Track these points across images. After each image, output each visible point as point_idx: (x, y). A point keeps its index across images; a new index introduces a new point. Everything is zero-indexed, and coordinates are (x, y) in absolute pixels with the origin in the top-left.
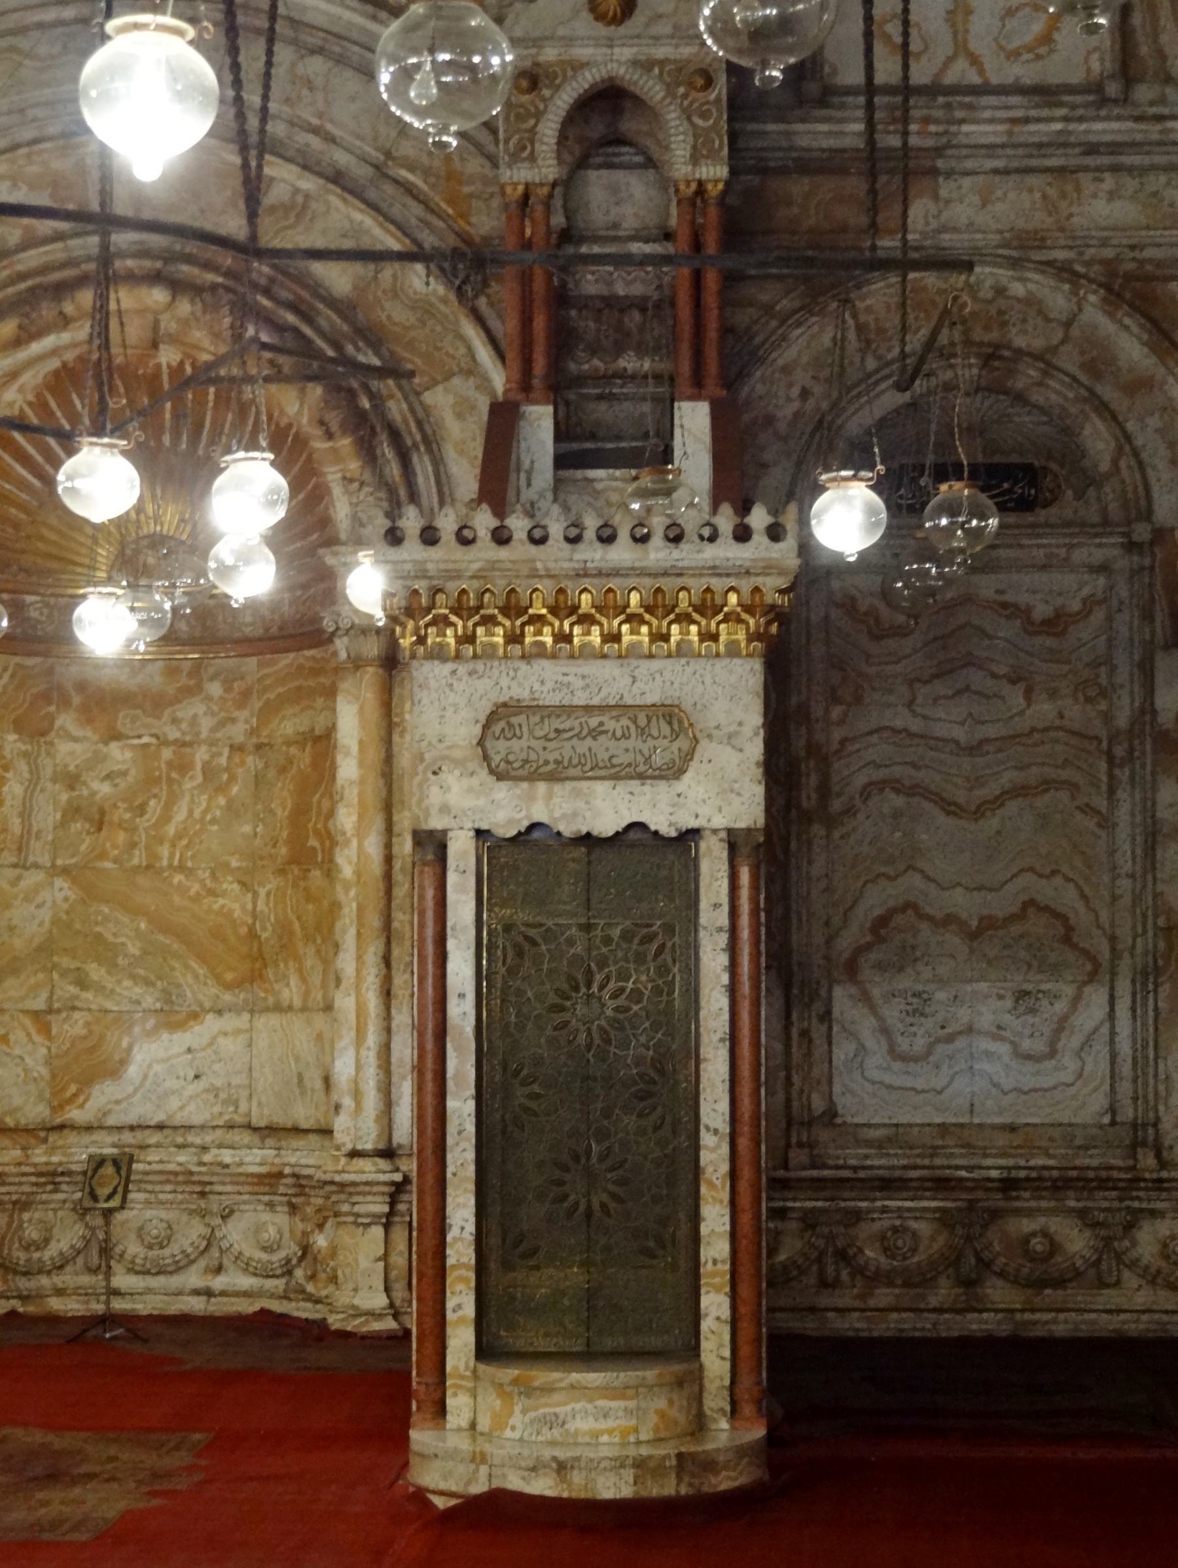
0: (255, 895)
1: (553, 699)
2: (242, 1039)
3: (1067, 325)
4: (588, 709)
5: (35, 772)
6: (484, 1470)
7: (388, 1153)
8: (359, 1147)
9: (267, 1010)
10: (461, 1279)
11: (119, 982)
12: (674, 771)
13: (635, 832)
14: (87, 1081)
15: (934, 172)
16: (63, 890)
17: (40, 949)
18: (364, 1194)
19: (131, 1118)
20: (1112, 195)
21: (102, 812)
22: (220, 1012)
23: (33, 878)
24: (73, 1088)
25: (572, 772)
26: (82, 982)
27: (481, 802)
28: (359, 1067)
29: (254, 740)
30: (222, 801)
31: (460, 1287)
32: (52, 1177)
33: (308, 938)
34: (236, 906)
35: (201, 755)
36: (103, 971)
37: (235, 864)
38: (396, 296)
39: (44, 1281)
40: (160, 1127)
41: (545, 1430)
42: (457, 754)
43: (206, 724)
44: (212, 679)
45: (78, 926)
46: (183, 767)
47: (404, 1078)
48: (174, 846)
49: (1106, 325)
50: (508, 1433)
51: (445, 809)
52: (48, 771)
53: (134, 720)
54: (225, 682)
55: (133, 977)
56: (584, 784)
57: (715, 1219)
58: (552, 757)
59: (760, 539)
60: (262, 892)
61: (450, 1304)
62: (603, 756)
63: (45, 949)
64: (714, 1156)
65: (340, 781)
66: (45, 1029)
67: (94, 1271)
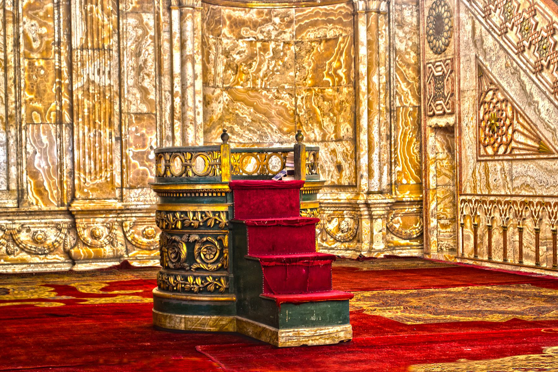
0: (296, 99)
7: (381, 192)
8: (373, 190)
11: (244, 132)
16: (226, 97)
18: (376, 207)
21: (237, 67)
23: (218, 91)
28: (370, 160)
29: (294, 40)
30: (281, 63)
33: (324, 115)
34: (288, 103)
35: (272, 45)
36: (239, 128)
37: (287, 86)
43: (274, 34)
44: (276, 16)
45: (230, 110)
46: (265, 49)
47: (384, 165)
48: (262, 80)
52: (220, 51)
54: (281, 18)
55: (250, 130)
60: (299, 97)
65: (360, 56)
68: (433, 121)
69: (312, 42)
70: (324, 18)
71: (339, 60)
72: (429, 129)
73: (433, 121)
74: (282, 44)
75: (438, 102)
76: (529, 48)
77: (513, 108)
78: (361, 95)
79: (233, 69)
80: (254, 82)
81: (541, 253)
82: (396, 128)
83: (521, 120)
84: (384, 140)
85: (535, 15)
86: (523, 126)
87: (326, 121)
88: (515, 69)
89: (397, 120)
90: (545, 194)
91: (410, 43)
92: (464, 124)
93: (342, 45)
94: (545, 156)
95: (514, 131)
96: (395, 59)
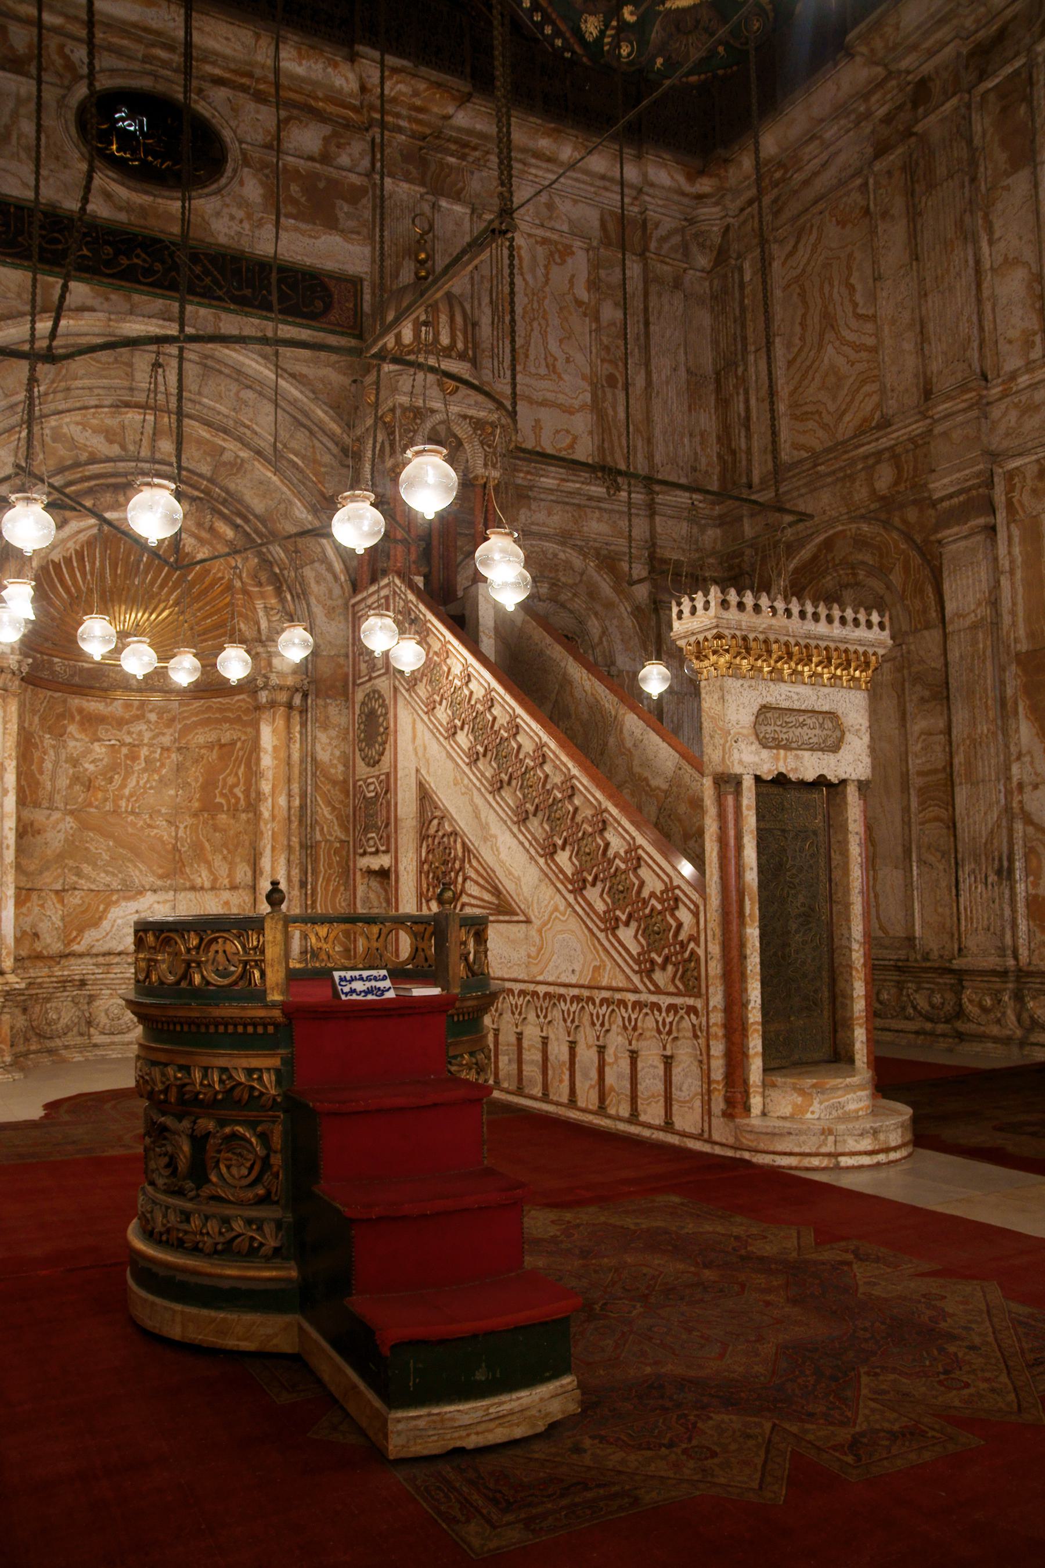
0: (177, 827)
1: (785, 704)
2: (168, 905)
3: (582, 574)
4: (799, 711)
5: (57, 754)
6: (831, 1139)
9: (185, 889)
10: (756, 1030)
12: (835, 748)
13: (821, 782)
14: (81, 931)
15: (528, 497)
16: (70, 823)
17: (58, 855)
19: (105, 948)
20: (599, 520)
21: (90, 781)
22: (155, 891)
23: (56, 815)
24: (74, 934)
25: (794, 745)
26: (79, 874)
27: (757, 759)
30: (156, 777)
31: (756, 1035)
32: (64, 983)
35: (144, 752)
37: (163, 811)
38: (286, 518)
39: (58, 1042)
40: (120, 954)
41: (834, 1113)
42: (745, 731)
43: (147, 736)
44: (151, 711)
46: (134, 757)
49: (597, 577)
50: (809, 1116)
51: (741, 762)
52: (63, 757)
53: (107, 731)
55: (107, 872)
56: (799, 752)
57: (859, 988)
58: (785, 736)
59: (876, 628)
60: (182, 826)
61: (751, 1045)
62: (806, 738)
63: (60, 857)
64: (858, 956)
66: (62, 901)
67: (82, 1035)
68: (364, 862)
69: (200, 748)
70: (218, 715)
71: (236, 774)
72: (358, 874)
73: (364, 862)
74: (159, 751)
75: (370, 835)
76: (485, 755)
77: (464, 844)
78: (262, 824)
79: (83, 784)
80: (115, 802)
81: (501, 1065)
82: (315, 872)
83: (475, 863)
84: (297, 887)
85: (492, 706)
86: (477, 871)
87: (218, 861)
88: (467, 787)
89: (315, 861)
90: (506, 976)
91: (337, 753)
92: (401, 868)
93: (241, 753)
94: (507, 918)
95: (465, 880)
96: (314, 775)
